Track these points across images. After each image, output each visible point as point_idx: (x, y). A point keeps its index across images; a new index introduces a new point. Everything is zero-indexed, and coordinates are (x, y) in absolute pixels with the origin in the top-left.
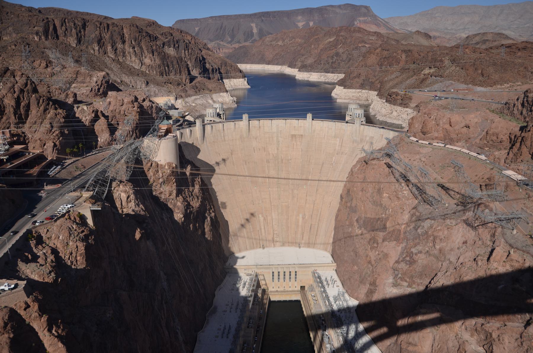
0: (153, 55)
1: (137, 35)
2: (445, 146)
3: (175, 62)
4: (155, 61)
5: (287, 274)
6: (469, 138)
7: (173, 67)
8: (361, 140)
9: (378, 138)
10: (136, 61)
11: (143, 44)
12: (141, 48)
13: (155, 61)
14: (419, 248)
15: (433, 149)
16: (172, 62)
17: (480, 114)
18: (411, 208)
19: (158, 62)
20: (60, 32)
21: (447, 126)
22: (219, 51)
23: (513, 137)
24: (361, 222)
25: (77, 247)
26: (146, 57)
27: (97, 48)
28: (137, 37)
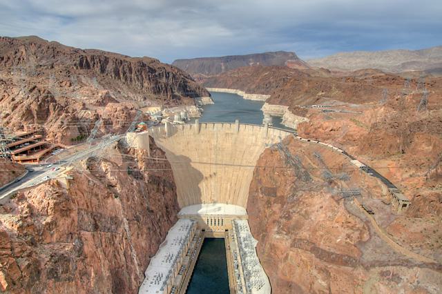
5: (217, 223)
9: (277, 135)
12: (142, 76)
14: (294, 209)
19: (153, 85)
20: (91, 64)
22: (197, 79)
24: (263, 189)
25: (49, 203)
27: (113, 76)
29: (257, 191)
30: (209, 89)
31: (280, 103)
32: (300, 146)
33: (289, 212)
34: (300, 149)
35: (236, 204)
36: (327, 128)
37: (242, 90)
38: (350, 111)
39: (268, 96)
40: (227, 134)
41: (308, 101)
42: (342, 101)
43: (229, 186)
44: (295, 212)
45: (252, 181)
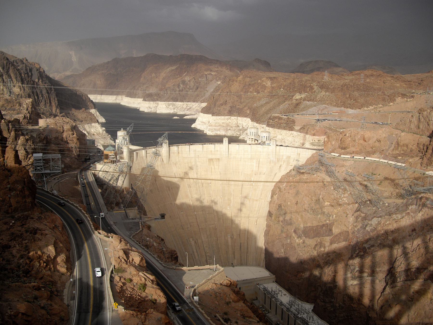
0: (22, 84)
1: (5, 62)
2: (365, 158)
3: (44, 92)
4: (24, 89)
6: (383, 151)
7: (42, 96)
8: (278, 160)
10: (5, 90)
11: (11, 71)
12: (10, 77)
13: (24, 89)
15: (355, 161)
16: (41, 92)
17: (385, 130)
18: (353, 212)
21: (362, 142)
23: (422, 147)
26: (14, 86)
28: (5, 64)
29: (288, 236)
30: (95, 98)
31: (230, 113)
32: (343, 166)
33: (365, 248)
34: (344, 169)
35: (246, 265)
36: (369, 140)
37: (131, 95)
38: (349, 120)
39: (204, 105)
40: (211, 160)
41: (281, 106)
42: (335, 106)
43: (230, 240)
44: (373, 246)
45: (268, 226)
